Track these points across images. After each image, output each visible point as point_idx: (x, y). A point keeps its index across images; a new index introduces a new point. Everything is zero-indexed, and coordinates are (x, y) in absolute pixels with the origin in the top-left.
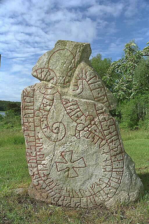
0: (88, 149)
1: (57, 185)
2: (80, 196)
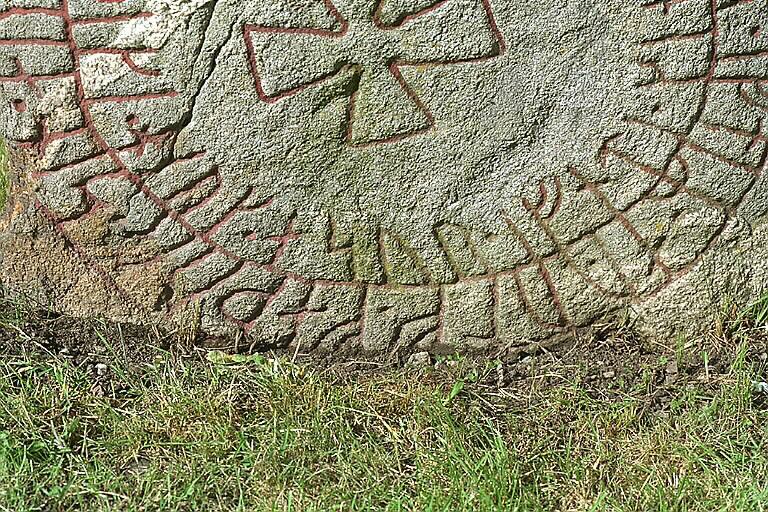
1: (247, 202)
2: (436, 266)
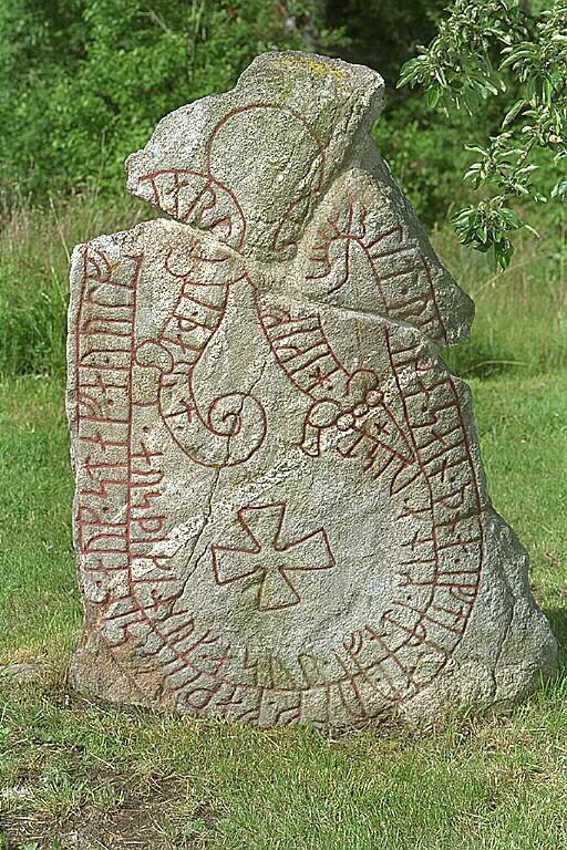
0: (346, 495)
1: (206, 640)
2: (300, 681)
